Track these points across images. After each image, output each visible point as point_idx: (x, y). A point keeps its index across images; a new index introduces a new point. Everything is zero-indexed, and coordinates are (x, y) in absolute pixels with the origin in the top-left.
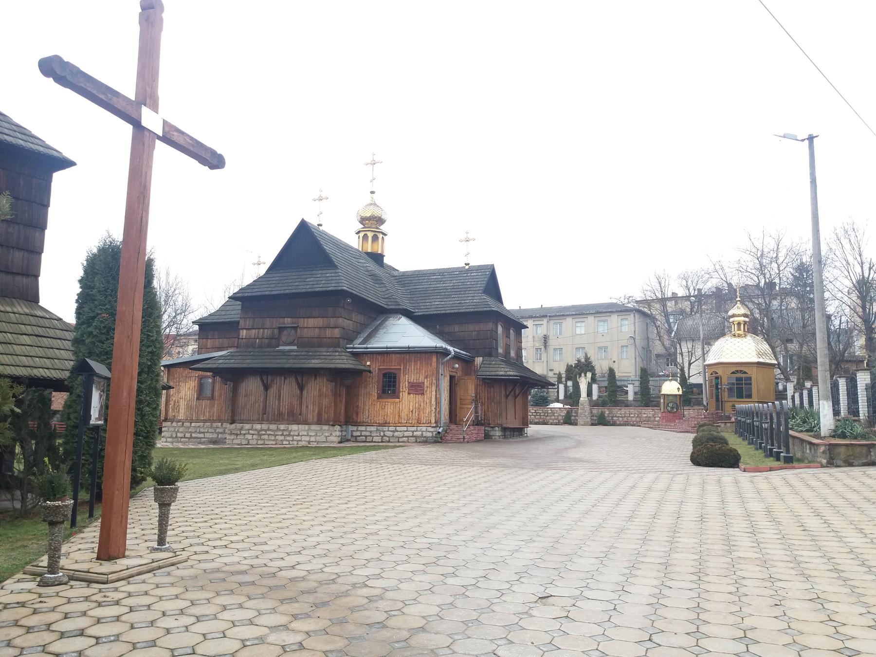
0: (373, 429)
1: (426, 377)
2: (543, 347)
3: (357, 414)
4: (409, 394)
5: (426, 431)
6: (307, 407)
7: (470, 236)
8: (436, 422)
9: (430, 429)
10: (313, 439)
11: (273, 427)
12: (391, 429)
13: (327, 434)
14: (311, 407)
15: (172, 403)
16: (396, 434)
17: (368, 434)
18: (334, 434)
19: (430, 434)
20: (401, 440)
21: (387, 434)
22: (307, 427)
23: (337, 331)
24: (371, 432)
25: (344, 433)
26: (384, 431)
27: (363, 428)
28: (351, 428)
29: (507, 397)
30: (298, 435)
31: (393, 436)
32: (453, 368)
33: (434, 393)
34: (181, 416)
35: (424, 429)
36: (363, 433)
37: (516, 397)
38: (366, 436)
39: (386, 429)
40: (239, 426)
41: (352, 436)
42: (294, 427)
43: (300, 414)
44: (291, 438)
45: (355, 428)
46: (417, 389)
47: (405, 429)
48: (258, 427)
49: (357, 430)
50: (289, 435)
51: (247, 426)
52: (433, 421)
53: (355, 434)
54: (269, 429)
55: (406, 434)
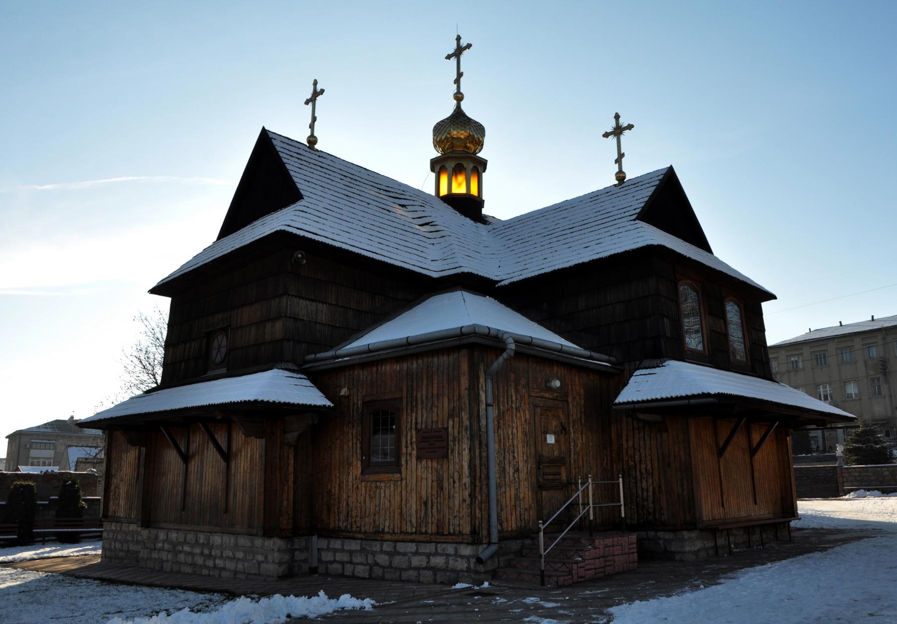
0: (354, 545)
1: (451, 415)
2: (880, 376)
3: (329, 510)
4: (419, 458)
5: (457, 555)
6: (235, 496)
7: (624, 122)
8: (474, 532)
9: (466, 551)
10: (240, 566)
11: (191, 537)
12: (387, 547)
13: (260, 558)
14: (239, 495)
15: (112, 488)
16: (397, 561)
17: (345, 557)
18: (270, 559)
19: (462, 565)
20: (405, 575)
21: (383, 559)
22: (233, 538)
23: (279, 325)
24: (351, 552)
25: (299, 556)
26: (374, 553)
27: (337, 544)
28: (317, 542)
29: (721, 452)
30: (221, 557)
31: (390, 566)
32: (550, 389)
33: (466, 453)
34: (121, 514)
35: (450, 549)
36: (339, 557)
37: (753, 451)
38: (342, 563)
39: (376, 546)
40: (154, 532)
41: (320, 560)
42: (217, 539)
43: (226, 511)
44: (210, 563)
45: (323, 543)
46: (434, 445)
47: (412, 547)
48: (174, 535)
49: (328, 549)
50: (210, 556)
51: (162, 535)
52: (467, 530)
53: (327, 556)
54: (185, 542)
55: (416, 561)
